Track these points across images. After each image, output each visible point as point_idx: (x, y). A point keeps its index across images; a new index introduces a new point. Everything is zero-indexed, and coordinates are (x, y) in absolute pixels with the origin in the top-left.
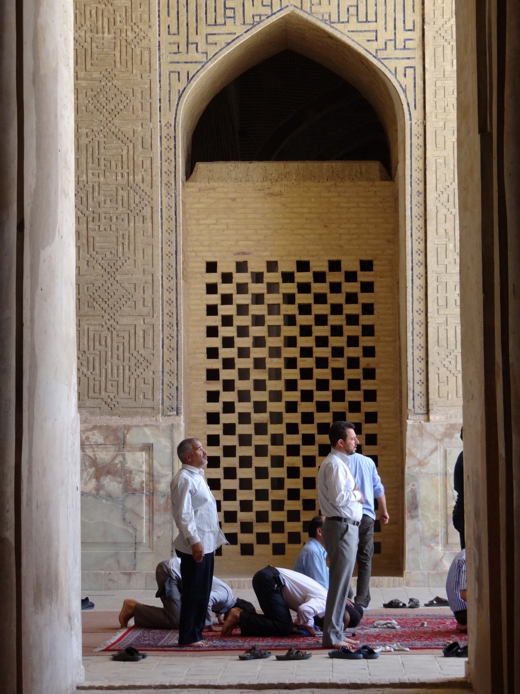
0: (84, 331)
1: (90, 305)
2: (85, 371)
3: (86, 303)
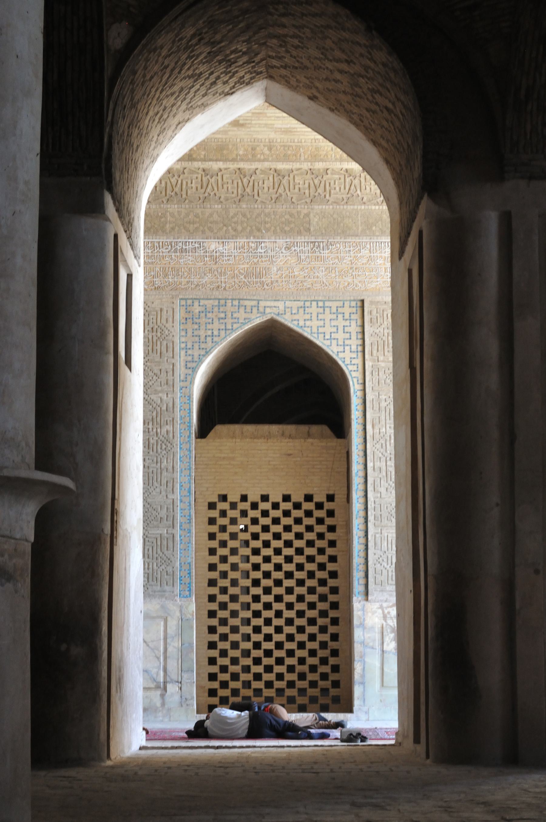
0: (385, 537)
1: (389, 519)
2: (386, 565)
3: (386, 518)
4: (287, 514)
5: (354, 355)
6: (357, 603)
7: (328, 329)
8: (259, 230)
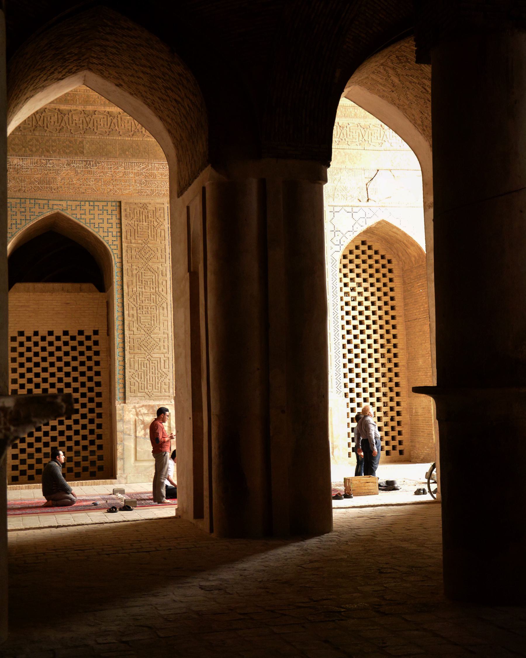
4: (66, 343)
5: (115, 239)
6: (119, 405)
7: (97, 221)
8: (48, 151)
